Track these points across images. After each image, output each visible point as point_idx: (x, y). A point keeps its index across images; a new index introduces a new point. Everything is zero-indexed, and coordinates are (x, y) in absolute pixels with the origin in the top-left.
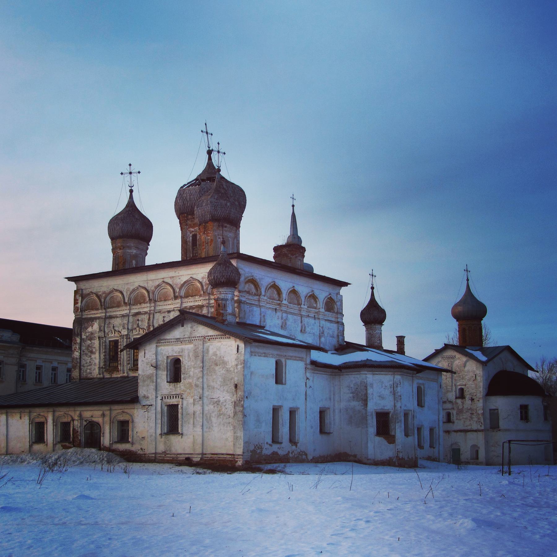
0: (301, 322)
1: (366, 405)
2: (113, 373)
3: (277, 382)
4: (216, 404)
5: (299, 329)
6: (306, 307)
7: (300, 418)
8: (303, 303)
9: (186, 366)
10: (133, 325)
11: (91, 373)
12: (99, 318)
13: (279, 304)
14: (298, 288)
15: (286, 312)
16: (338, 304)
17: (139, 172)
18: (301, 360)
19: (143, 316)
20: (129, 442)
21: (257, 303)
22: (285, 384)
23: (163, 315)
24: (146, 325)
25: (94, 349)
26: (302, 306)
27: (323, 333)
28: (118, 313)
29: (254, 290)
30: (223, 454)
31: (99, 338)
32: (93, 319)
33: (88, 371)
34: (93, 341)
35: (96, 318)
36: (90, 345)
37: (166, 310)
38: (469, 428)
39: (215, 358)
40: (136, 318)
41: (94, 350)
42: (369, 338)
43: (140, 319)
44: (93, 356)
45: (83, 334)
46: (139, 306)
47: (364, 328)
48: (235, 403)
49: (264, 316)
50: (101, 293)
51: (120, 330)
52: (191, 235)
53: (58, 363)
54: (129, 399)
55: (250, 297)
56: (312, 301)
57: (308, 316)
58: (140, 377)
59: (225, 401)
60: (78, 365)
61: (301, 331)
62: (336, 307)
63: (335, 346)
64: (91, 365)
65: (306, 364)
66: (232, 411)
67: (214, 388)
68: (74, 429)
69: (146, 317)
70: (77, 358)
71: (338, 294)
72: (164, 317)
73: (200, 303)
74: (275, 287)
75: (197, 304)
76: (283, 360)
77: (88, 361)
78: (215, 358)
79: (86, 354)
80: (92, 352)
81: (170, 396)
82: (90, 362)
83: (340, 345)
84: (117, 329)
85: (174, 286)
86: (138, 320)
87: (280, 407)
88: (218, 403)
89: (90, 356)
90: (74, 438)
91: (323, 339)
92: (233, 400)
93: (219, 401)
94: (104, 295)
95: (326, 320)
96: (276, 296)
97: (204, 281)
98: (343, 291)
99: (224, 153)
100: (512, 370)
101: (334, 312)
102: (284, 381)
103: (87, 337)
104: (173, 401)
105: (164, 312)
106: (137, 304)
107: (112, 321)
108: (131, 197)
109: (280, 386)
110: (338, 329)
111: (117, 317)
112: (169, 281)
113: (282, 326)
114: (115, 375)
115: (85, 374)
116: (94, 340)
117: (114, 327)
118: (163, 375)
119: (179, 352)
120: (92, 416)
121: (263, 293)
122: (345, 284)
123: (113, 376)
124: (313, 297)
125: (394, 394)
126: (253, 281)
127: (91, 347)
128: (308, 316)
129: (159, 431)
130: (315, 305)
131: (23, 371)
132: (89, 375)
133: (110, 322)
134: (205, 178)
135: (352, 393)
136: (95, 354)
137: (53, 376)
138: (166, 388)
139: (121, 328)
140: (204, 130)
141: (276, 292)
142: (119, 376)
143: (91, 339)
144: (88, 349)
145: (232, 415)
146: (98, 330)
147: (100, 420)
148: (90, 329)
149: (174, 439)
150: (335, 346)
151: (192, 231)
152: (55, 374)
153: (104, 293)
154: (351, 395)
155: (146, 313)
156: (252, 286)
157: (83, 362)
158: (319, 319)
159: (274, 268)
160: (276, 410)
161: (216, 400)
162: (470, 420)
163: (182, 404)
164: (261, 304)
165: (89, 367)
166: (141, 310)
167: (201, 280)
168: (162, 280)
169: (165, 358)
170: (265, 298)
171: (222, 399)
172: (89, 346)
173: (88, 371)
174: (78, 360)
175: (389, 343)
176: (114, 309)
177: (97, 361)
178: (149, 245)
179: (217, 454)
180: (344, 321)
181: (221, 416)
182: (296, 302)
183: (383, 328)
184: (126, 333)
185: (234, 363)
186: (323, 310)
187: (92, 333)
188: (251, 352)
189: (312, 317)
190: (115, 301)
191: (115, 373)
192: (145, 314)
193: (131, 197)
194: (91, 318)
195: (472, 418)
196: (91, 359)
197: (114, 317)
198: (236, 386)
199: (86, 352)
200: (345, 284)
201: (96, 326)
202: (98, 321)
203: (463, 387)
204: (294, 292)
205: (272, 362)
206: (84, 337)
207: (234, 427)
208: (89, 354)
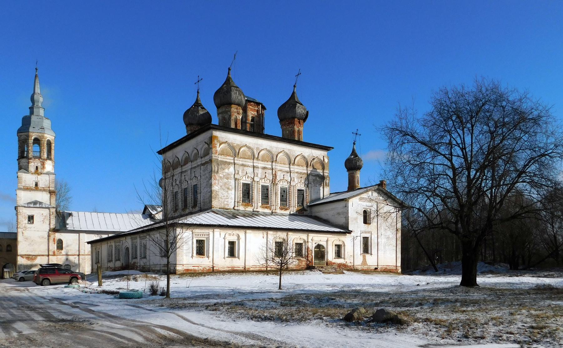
4: (387, 239)
11: (228, 205)
23: (284, 173)
25: (230, 187)
30: (391, 266)
36: (227, 183)
37: (285, 171)
40: (265, 171)
41: (230, 187)
44: (230, 192)
46: (266, 163)
77: (225, 195)
80: (228, 189)
81: (365, 232)
82: (227, 196)
84: (250, 175)
89: (227, 192)
107: (246, 168)
111: (249, 167)
115: (222, 204)
120: (320, 241)
132: (226, 206)
133: (244, 169)
136: (231, 190)
144: (225, 186)
147: (323, 243)
148: (226, 171)
149: (368, 256)
153: (238, 145)
157: (220, 195)
168: (283, 150)
172: (226, 183)
173: (226, 203)
176: (246, 160)
179: (389, 266)
181: (391, 246)
187: (228, 174)
190: (247, 154)
194: (226, 162)
196: (228, 194)
197: (247, 166)
199: (223, 187)
208: (226, 190)
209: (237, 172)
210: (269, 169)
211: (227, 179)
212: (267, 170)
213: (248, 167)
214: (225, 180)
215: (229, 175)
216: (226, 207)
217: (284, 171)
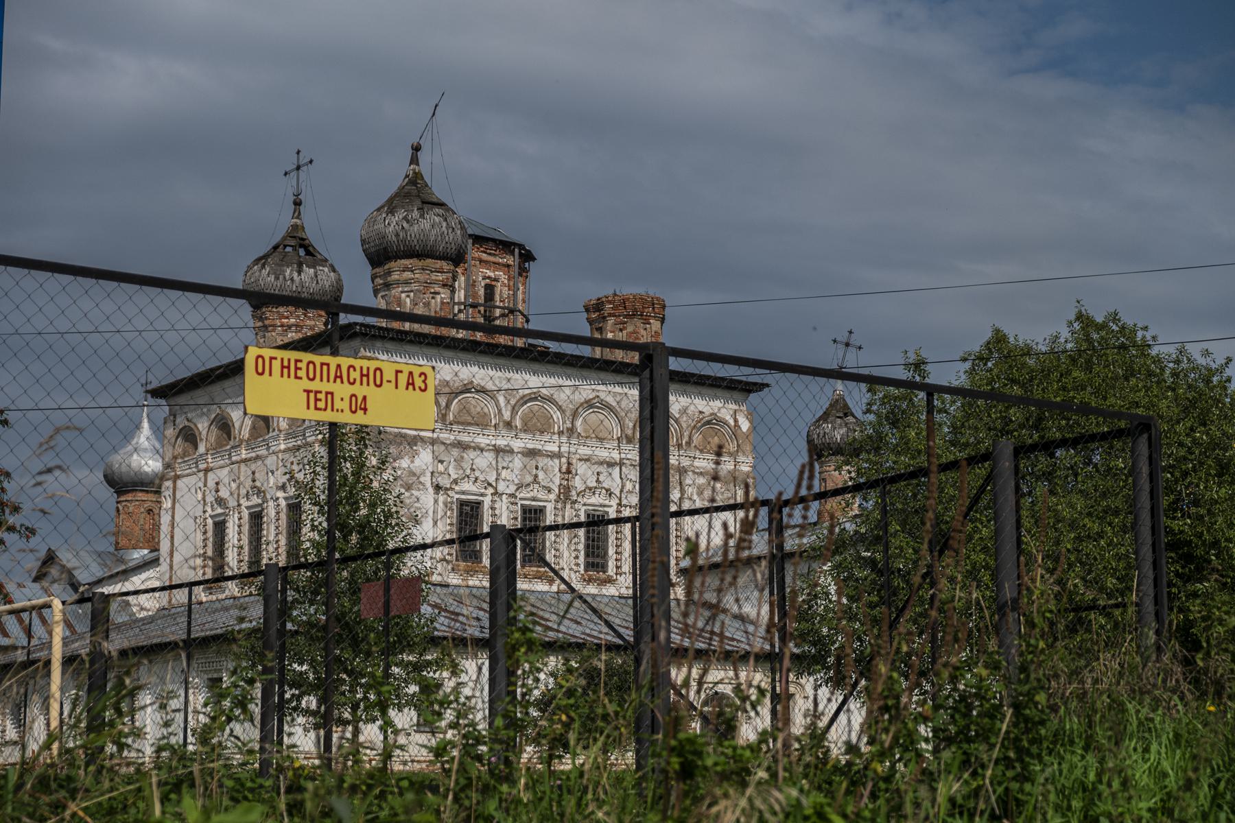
2: (472, 576)
12: (433, 442)
28: (482, 441)
34: (413, 492)
43: (540, 465)
51: (492, 479)
52: (483, 284)
72: (598, 474)
86: (537, 468)
105: (601, 463)
108: (414, 160)
112: (610, 400)
116: (419, 490)
148: (404, 463)
151: (489, 278)
167: (677, 416)
184: (512, 489)
215: (414, 474)
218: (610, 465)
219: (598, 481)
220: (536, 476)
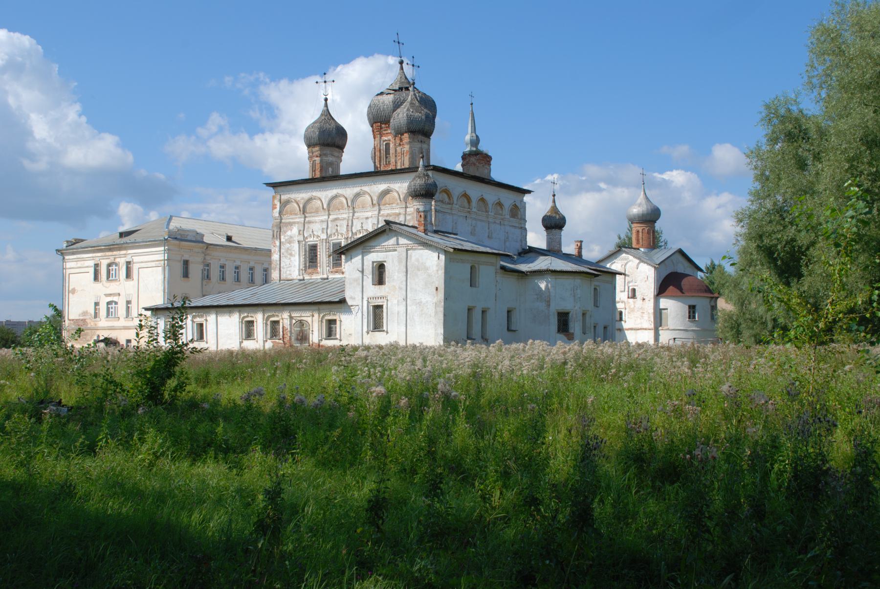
0: (489, 228)
1: (549, 305)
3: (471, 286)
5: (487, 235)
6: (493, 214)
7: (490, 316)
8: (490, 211)
9: (391, 271)
10: (331, 230)
11: (291, 274)
12: (298, 223)
13: (469, 212)
14: (486, 197)
15: (475, 219)
16: (522, 210)
17: (333, 81)
18: (492, 265)
19: (341, 222)
20: (337, 339)
21: (449, 211)
22: (478, 287)
24: (345, 230)
26: (490, 213)
27: (508, 238)
29: (447, 200)
31: (298, 242)
32: (291, 224)
33: (288, 272)
34: (292, 244)
35: (294, 223)
38: (639, 326)
39: (417, 263)
40: (335, 224)
41: (293, 253)
42: (549, 243)
44: (292, 259)
45: (282, 237)
47: (545, 233)
48: (436, 304)
49: (456, 223)
50: (299, 199)
52: (384, 143)
53: (241, 262)
54: (337, 300)
55: (444, 206)
56: (499, 208)
57: (495, 222)
58: (347, 280)
59: (427, 302)
60: (278, 266)
61: (488, 237)
62: (519, 213)
63: (518, 250)
64: (291, 267)
65: (496, 269)
66: (433, 311)
67: (416, 290)
68: (283, 327)
69: (345, 223)
70: (276, 261)
71: (522, 201)
72: (362, 223)
73: (397, 211)
74: (466, 196)
75: (394, 211)
76: (477, 266)
78: (417, 263)
79: (286, 257)
80: (291, 255)
83: (523, 249)
85: (372, 195)
86: (337, 226)
87: (474, 307)
88: (420, 303)
89: (290, 259)
90: (283, 335)
91: (507, 244)
92: (434, 301)
93: (421, 302)
94: (302, 201)
95: (510, 226)
96: (466, 204)
97: (401, 190)
98: (527, 198)
99: (419, 67)
100: (683, 272)
101: (518, 218)
102: (477, 286)
103: (286, 240)
104: (378, 302)
106: (335, 210)
108: (326, 105)
109: (474, 289)
110: (521, 234)
111: (316, 222)
113: (471, 233)
114: (314, 277)
117: (313, 232)
118: (369, 279)
119: (384, 258)
121: (455, 202)
122: (529, 192)
123: (313, 278)
124: (500, 204)
125: (574, 296)
126: (446, 191)
127: (290, 250)
128: (495, 222)
129: (365, 329)
130: (501, 212)
131: (208, 270)
134: (397, 88)
135: (537, 295)
137: (250, 276)
138: (372, 290)
139: (320, 232)
140: (401, 45)
141: (466, 201)
142: (319, 277)
143: (290, 243)
144: (287, 252)
145: (433, 314)
146: (297, 234)
148: (289, 233)
150: (518, 250)
151: (386, 140)
152: (223, 271)
154: (536, 297)
155: (344, 219)
156: (446, 195)
158: (504, 225)
159: (465, 178)
160: (470, 310)
161: (418, 301)
162: (641, 319)
163: (387, 305)
164: (453, 212)
165: (289, 269)
166: (340, 216)
167: (397, 190)
169: (371, 263)
170: (457, 206)
171: (424, 301)
172: (288, 248)
173: (288, 272)
174: (278, 263)
175: (569, 248)
177: (297, 263)
178: (343, 152)
180: (527, 227)
181: (424, 315)
182: (484, 210)
183: (563, 233)
185: (435, 268)
186: (508, 217)
187: (291, 237)
188: (450, 259)
189: (498, 224)
191: (315, 275)
192: (343, 220)
193: (326, 105)
195: (642, 317)
197: (313, 222)
198: (437, 289)
199: (286, 254)
200: (529, 192)
201: (295, 230)
202: (297, 225)
203: (634, 287)
204: (482, 200)
205: (468, 267)
206: (282, 240)
207: (435, 325)
208: (289, 256)
209: (301, 232)
210: (341, 220)
211: (290, 243)
212: (338, 221)
213: (314, 224)
214: (288, 245)
216: (289, 277)
217: (362, 217)
218: (367, 218)
219: (362, 227)
220: (337, 230)
